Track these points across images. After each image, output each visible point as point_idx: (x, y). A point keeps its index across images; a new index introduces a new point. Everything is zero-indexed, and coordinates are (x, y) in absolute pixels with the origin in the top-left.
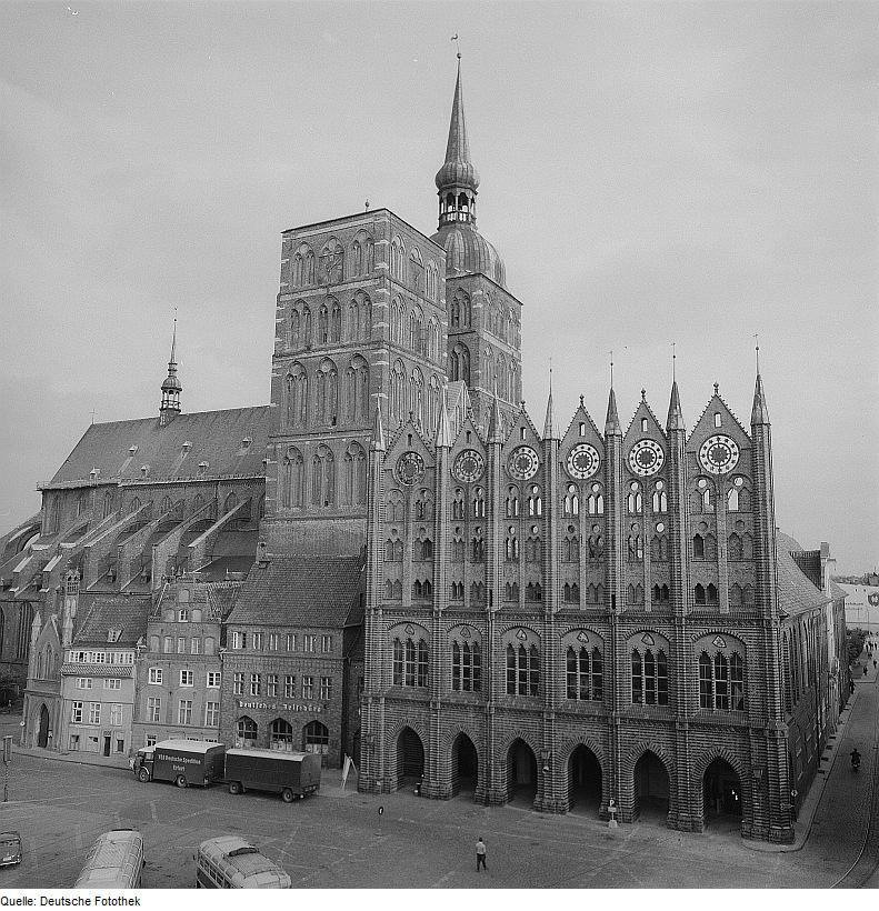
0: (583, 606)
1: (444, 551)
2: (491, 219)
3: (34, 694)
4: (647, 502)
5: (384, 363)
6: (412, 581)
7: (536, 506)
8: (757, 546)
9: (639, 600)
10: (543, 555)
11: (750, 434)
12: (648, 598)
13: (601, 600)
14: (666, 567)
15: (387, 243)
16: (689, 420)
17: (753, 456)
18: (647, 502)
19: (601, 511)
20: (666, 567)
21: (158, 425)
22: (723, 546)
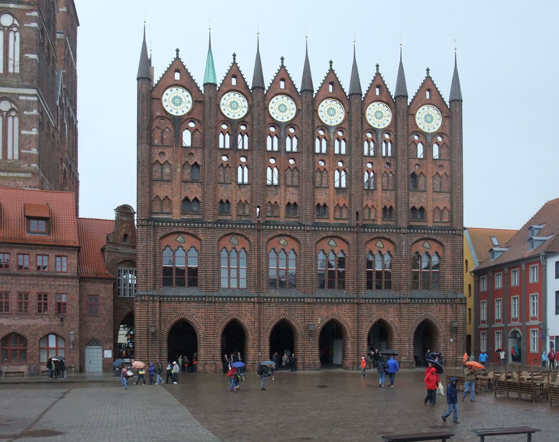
0: (332, 221)
9: (373, 216)
12: (380, 215)
13: (344, 216)
14: (393, 193)
20: (393, 193)
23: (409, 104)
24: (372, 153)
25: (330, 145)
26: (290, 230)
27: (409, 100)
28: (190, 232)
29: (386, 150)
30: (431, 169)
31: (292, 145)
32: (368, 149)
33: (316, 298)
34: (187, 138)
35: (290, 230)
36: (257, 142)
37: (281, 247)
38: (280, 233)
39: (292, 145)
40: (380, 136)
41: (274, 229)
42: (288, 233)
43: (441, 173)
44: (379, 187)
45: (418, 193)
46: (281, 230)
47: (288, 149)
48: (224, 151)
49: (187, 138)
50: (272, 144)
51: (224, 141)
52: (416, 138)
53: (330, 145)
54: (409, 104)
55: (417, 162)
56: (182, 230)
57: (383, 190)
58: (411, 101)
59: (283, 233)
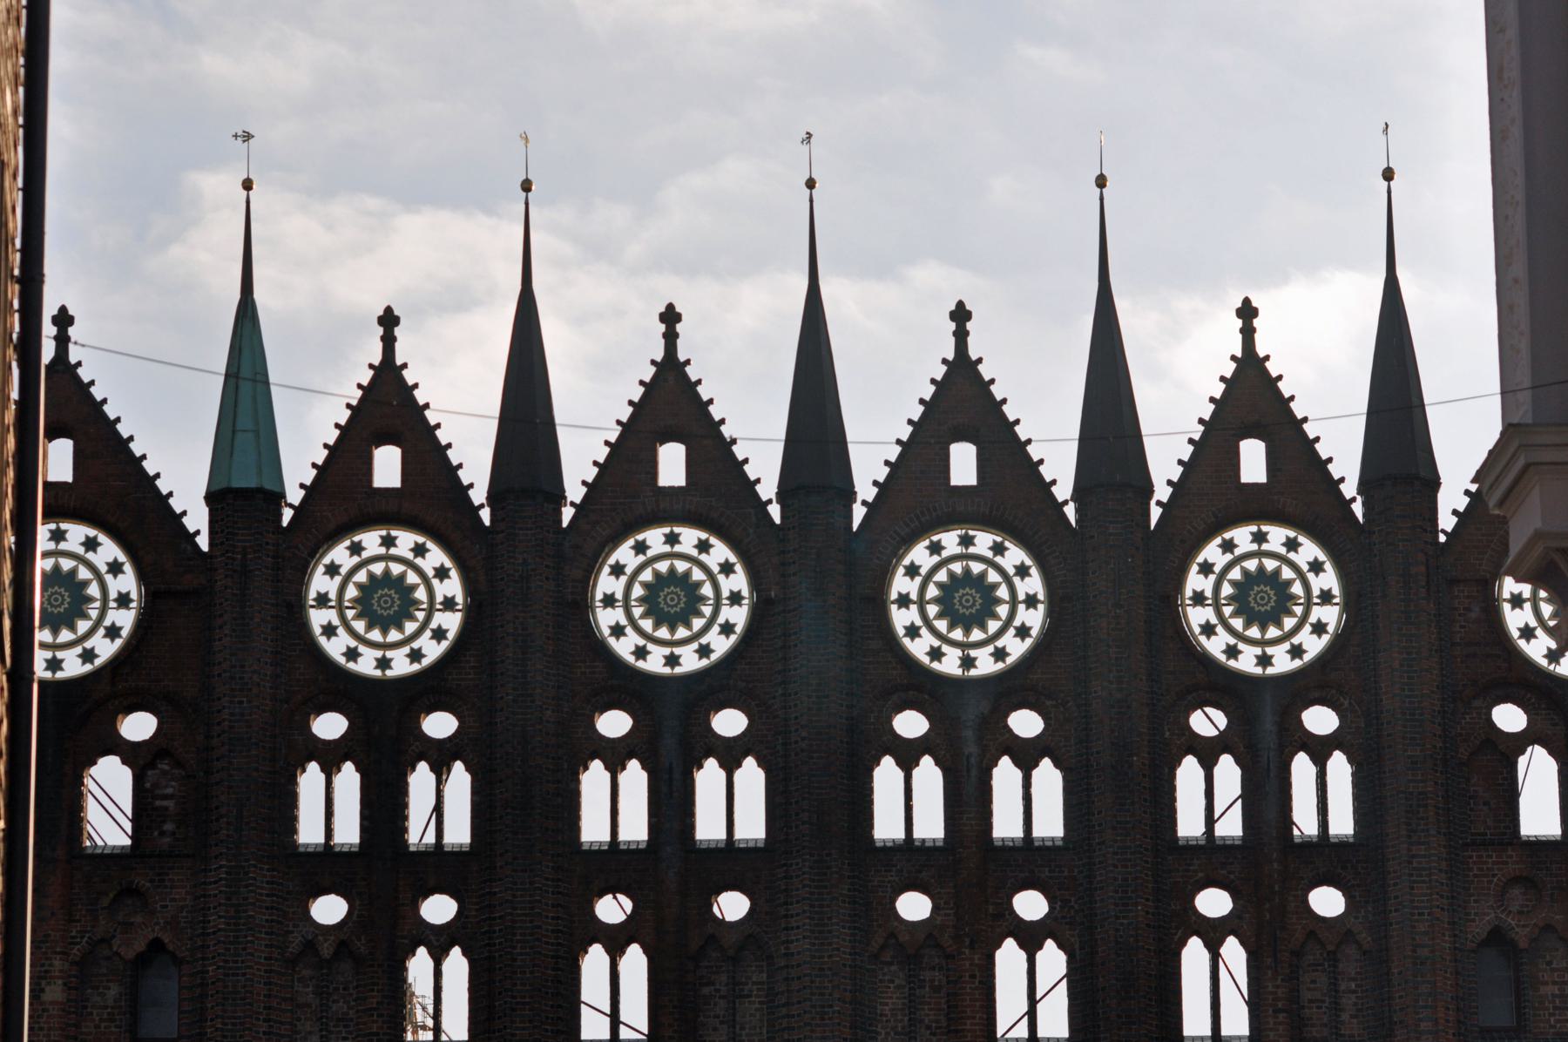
23: (1447, 522)
24: (1231, 826)
25: (968, 800)
27: (1451, 500)
29: (1324, 798)
31: (732, 804)
32: (1206, 800)
34: (109, 803)
36: (523, 803)
39: (732, 804)
40: (1268, 723)
47: (709, 827)
48: (328, 869)
49: (109, 803)
50: (612, 806)
51: (328, 808)
52: (1509, 718)
53: (968, 800)
54: (1447, 522)
58: (1462, 503)
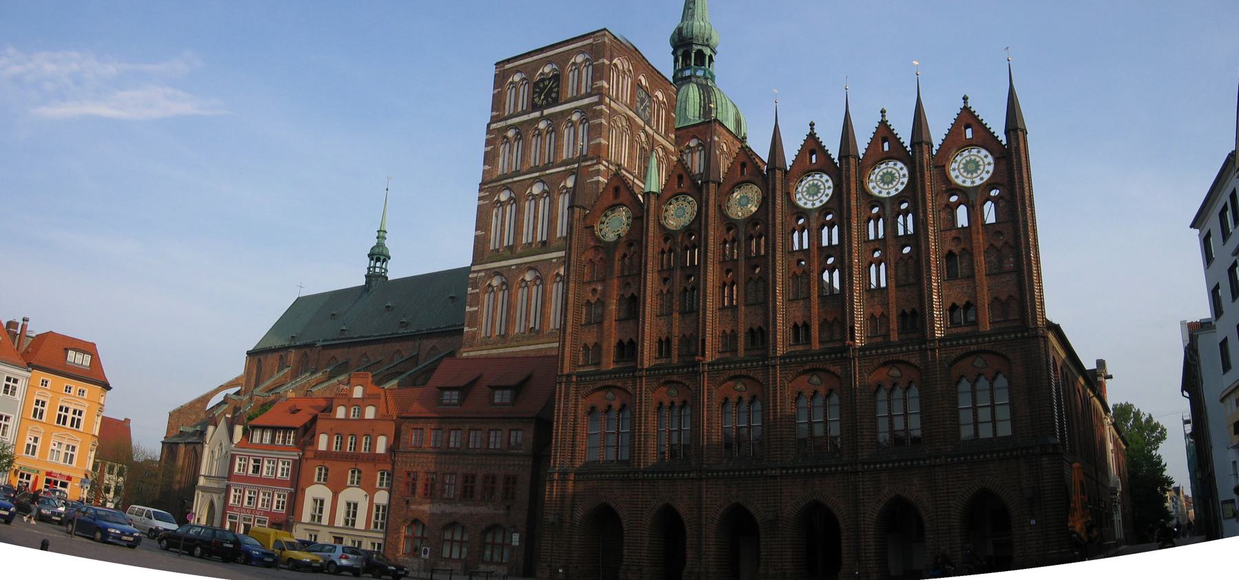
1: (650, 306)
2: (722, 70)
3: (204, 489)
4: (891, 226)
5: (601, 179)
6: (614, 342)
7: (758, 245)
8: (1018, 257)
10: (766, 297)
11: (1004, 142)
15: (607, 62)
16: (937, 133)
17: (1010, 163)
18: (891, 226)
19: (835, 241)
21: (365, 289)
22: (981, 261)
26: (746, 368)
28: (619, 384)
30: (980, 240)
33: (787, 469)
35: (746, 368)
37: (738, 394)
38: (732, 374)
41: (724, 369)
42: (743, 372)
43: (998, 244)
44: (892, 284)
45: (958, 282)
46: (735, 368)
55: (954, 233)
56: (610, 383)
57: (897, 286)
59: (738, 373)
